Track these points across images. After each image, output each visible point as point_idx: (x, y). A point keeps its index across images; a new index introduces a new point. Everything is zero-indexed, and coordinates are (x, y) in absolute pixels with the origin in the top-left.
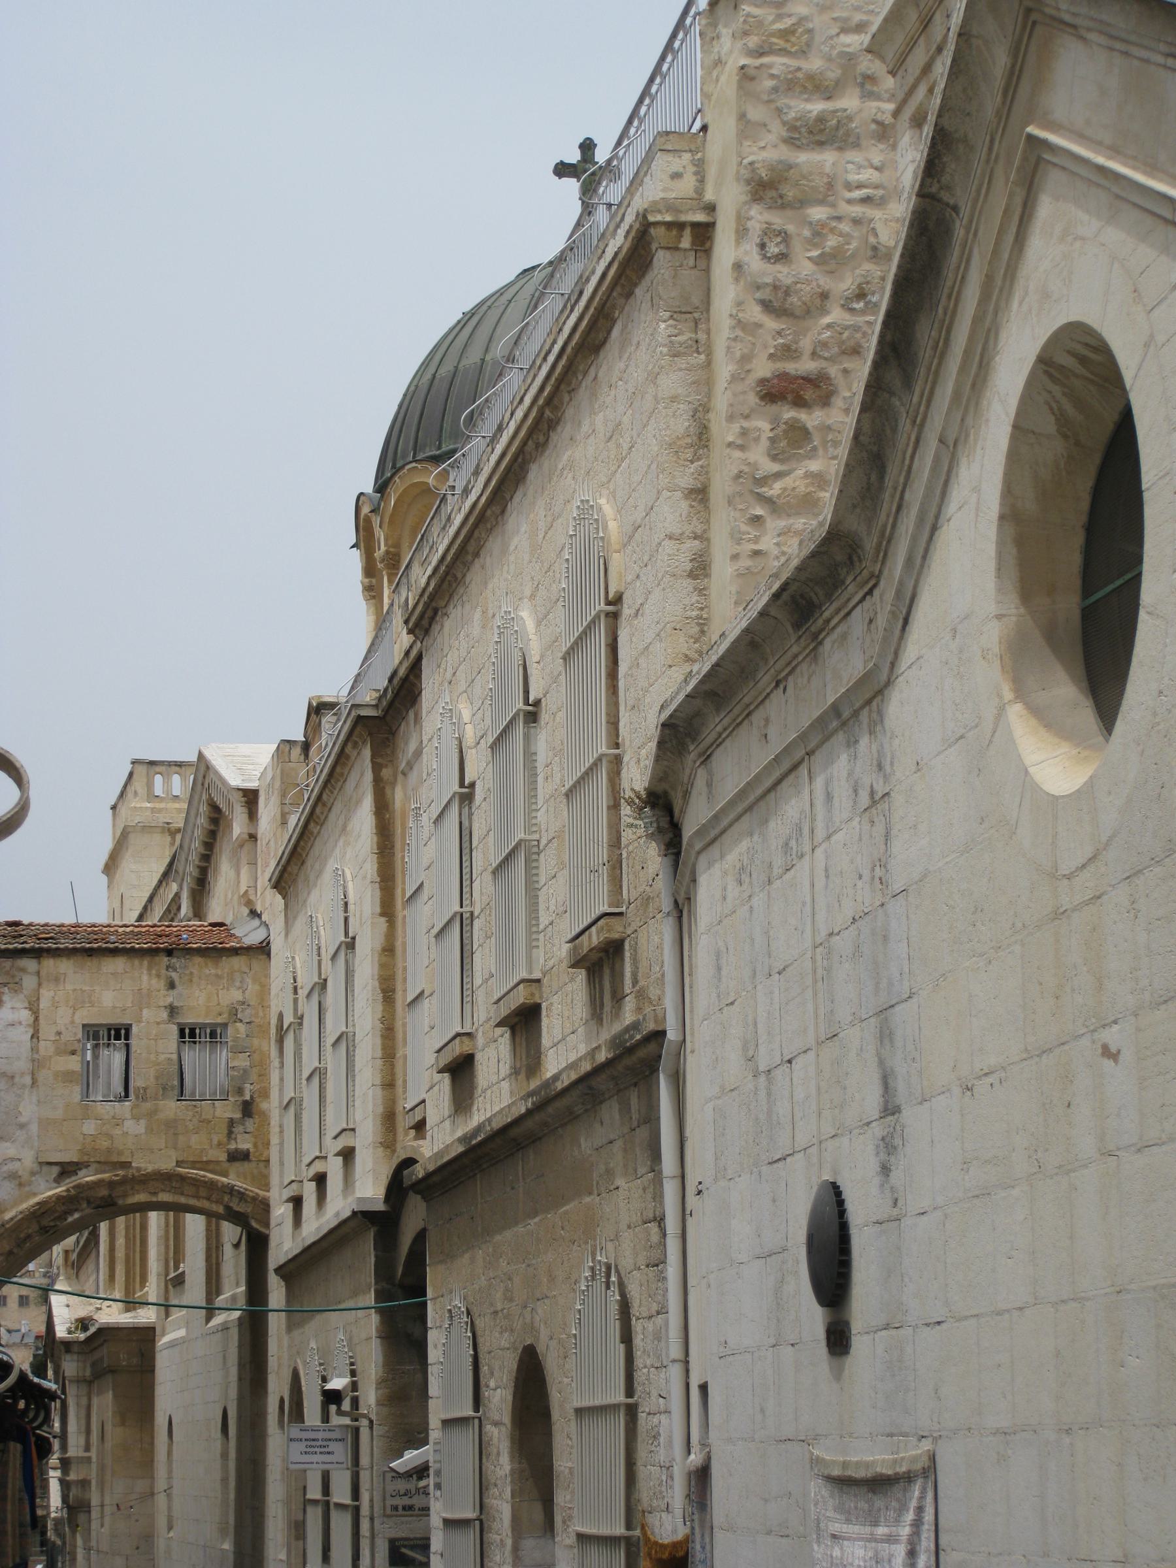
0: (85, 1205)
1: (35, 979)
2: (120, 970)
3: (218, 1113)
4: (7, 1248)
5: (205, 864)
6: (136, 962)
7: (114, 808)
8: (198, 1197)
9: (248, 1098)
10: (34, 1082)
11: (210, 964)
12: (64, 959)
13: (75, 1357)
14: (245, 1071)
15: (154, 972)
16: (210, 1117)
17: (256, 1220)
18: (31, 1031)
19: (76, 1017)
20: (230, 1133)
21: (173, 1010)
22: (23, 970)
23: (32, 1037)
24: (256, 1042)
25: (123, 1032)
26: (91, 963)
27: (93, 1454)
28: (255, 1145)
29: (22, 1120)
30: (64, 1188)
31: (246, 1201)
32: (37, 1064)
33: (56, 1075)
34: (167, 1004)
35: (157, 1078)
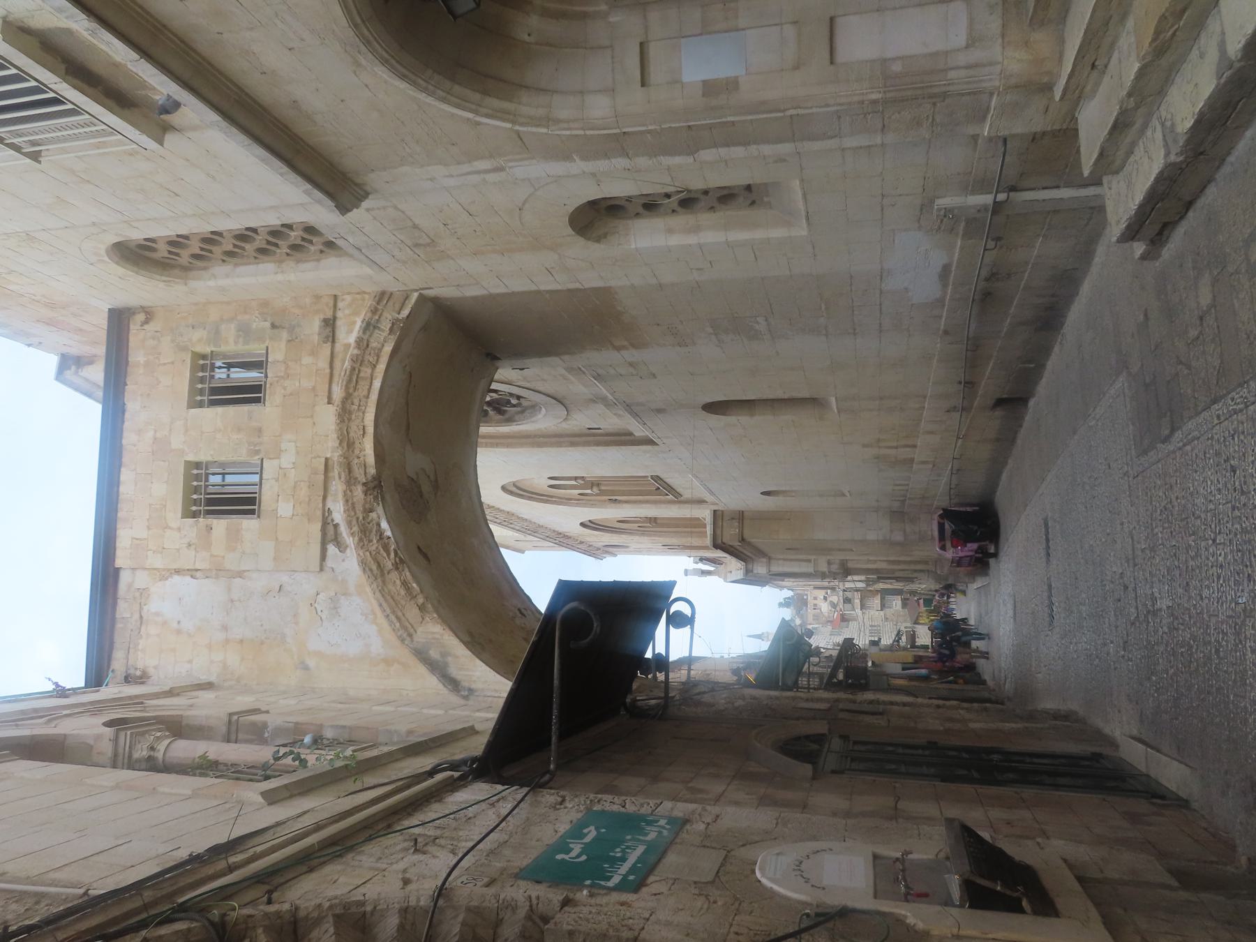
0: (373, 515)
1: (139, 573)
9: (268, 324)
10: (240, 574)
17: (401, 309)
22: (130, 586)
27: (812, 557)
31: (378, 321)
32: (217, 571)
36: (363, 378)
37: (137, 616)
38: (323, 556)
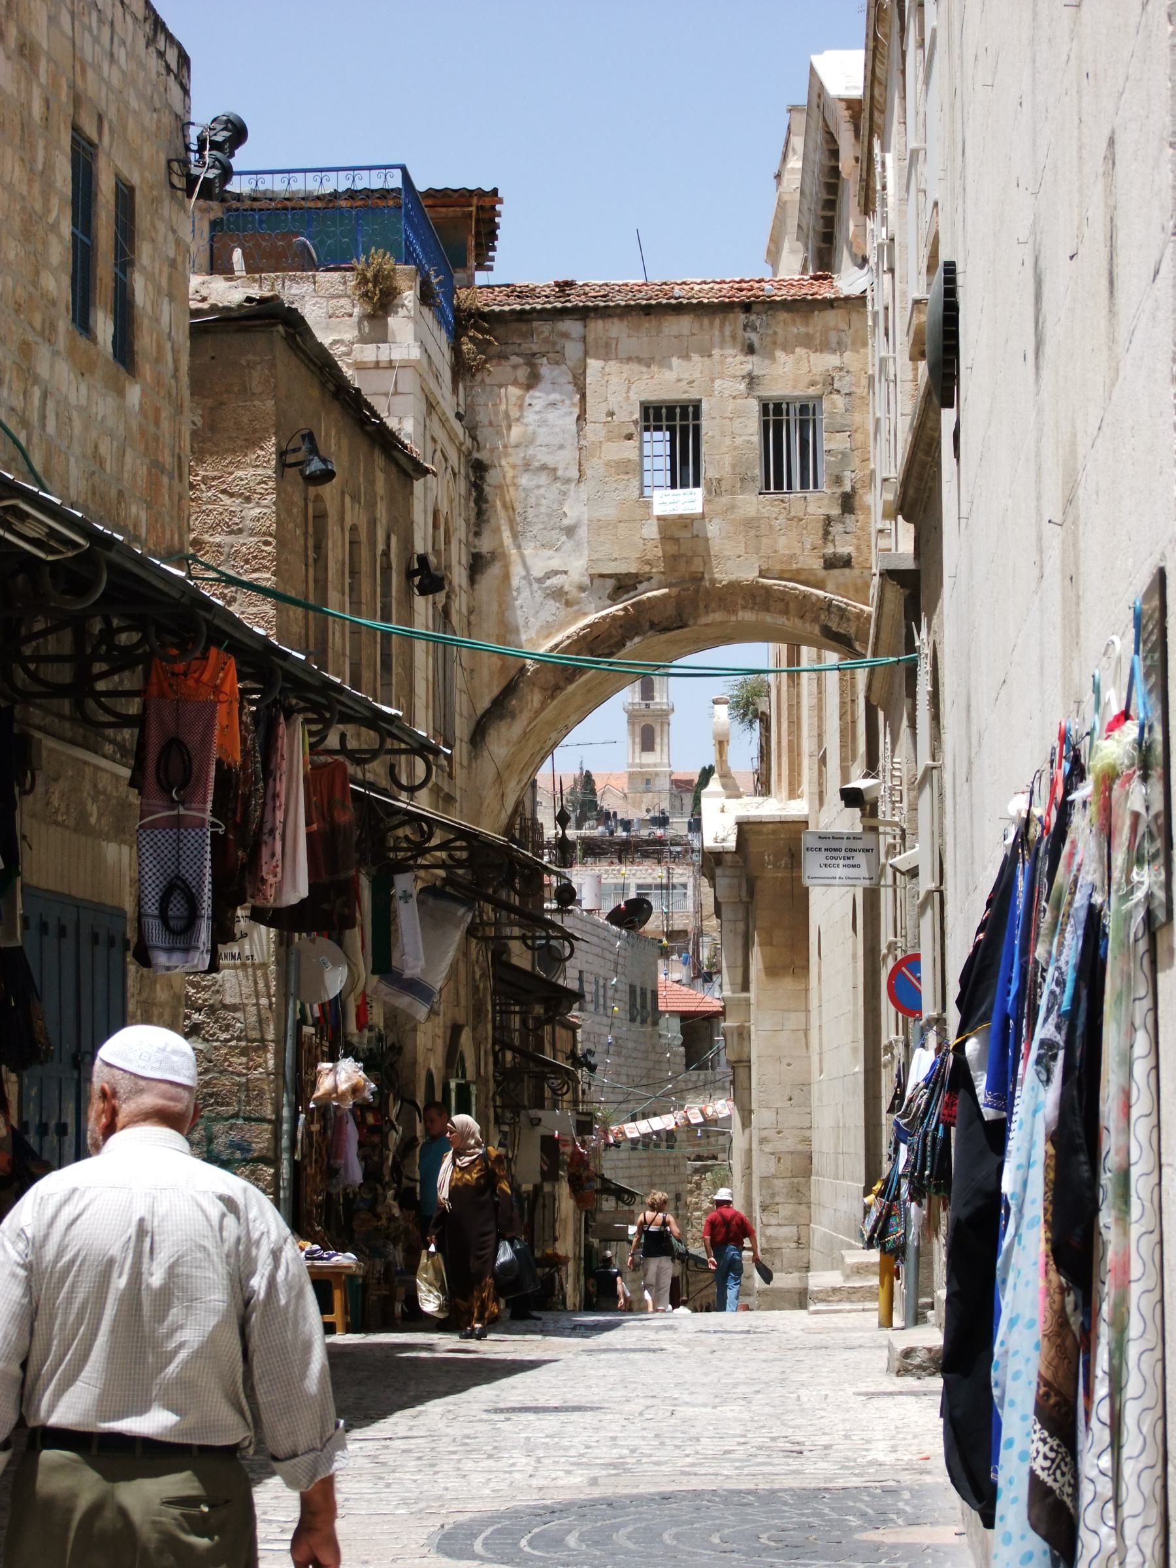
1: (580, 346)
2: (686, 332)
3: (811, 510)
4: (552, 681)
5: (830, 214)
6: (706, 321)
7: (778, 176)
8: (786, 612)
9: (848, 489)
11: (798, 320)
12: (616, 320)
13: (728, 872)
14: (844, 454)
15: (727, 333)
16: (801, 514)
18: (576, 411)
19: (631, 394)
20: (826, 533)
21: (752, 380)
22: (566, 335)
23: (579, 418)
24: (857, 417)
25: (691, 409)
26: (648, 324)
28: (858, 548)
29: (566, 522)
30: (621, 606)
33: (608, 464)
34: (744, 373)
35: (734, 466)
36: (787, 604)
37: (535, 348)
38: (602, 576)
